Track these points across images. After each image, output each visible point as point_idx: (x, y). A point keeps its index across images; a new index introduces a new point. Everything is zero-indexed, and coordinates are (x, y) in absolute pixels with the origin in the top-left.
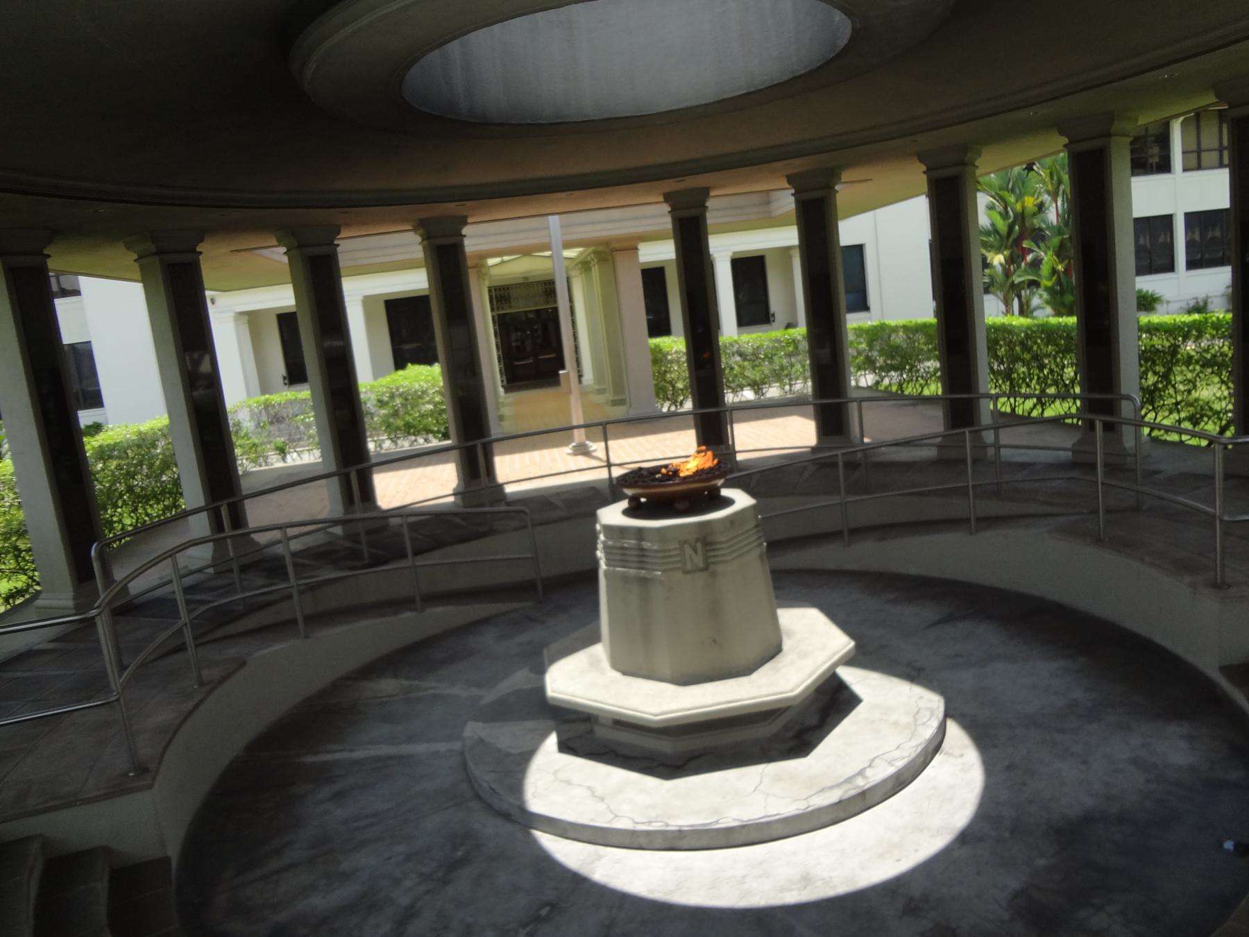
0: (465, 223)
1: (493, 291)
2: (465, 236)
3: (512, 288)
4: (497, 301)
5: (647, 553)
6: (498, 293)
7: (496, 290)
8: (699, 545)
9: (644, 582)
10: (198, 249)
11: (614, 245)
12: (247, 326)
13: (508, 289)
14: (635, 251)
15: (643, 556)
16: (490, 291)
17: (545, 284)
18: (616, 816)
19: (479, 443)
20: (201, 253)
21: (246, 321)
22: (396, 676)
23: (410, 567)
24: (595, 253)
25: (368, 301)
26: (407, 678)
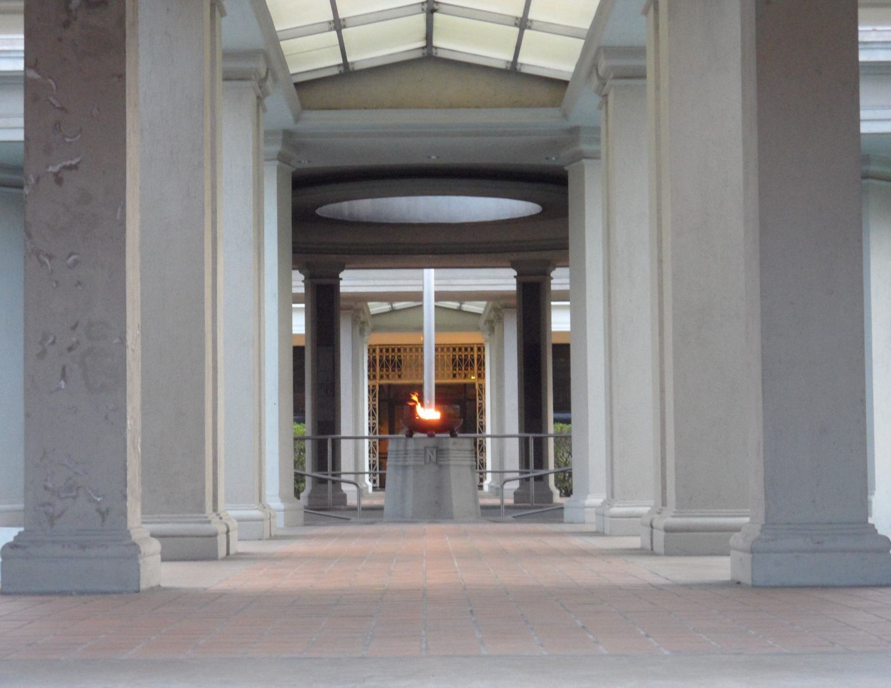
1: (378, 351)
2: (341, 279)
3: (405, 350)
4: (382, 367)
6: (384, 353)
7: (381, 351)
9: (405, 467)
13: (399, 350)
16: (372, 350)
17: (454, 349)
19: (329, 438)
24: (495, 309)
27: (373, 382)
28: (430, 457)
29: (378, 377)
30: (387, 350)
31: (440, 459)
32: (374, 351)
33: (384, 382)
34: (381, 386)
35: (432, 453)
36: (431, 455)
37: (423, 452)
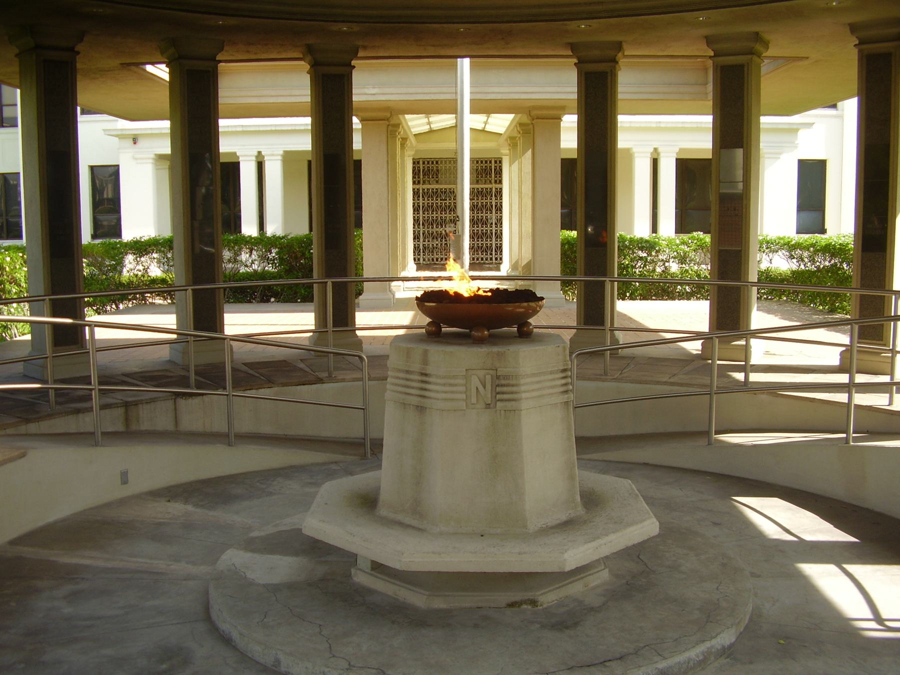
0: (355, 56)
2: (354, 67)
5: (431, 380)
7: (424, 163)
8: (488, 377)
10: (77, 49)
11: (534, 113)
12: (167, 171)
13: (437, 162)
14: (559, 120)
15: (426, 382)
16: (416, 162)
18: (334, 656)
20: (78, 53)
21: (168, 167)
22: (186, 502)
23: (227, 395)
25: (289, 158)
26: (196, 505)
27: (417, 187)
28: (477, 388)
29: (421, 182)
30: (428, 163)
31: (498, 397)
32: (418, 163)
33: (426, 186)
34: (423, 190)
35: (485, 387)
36: (481, 388)
37: (464, 396)
